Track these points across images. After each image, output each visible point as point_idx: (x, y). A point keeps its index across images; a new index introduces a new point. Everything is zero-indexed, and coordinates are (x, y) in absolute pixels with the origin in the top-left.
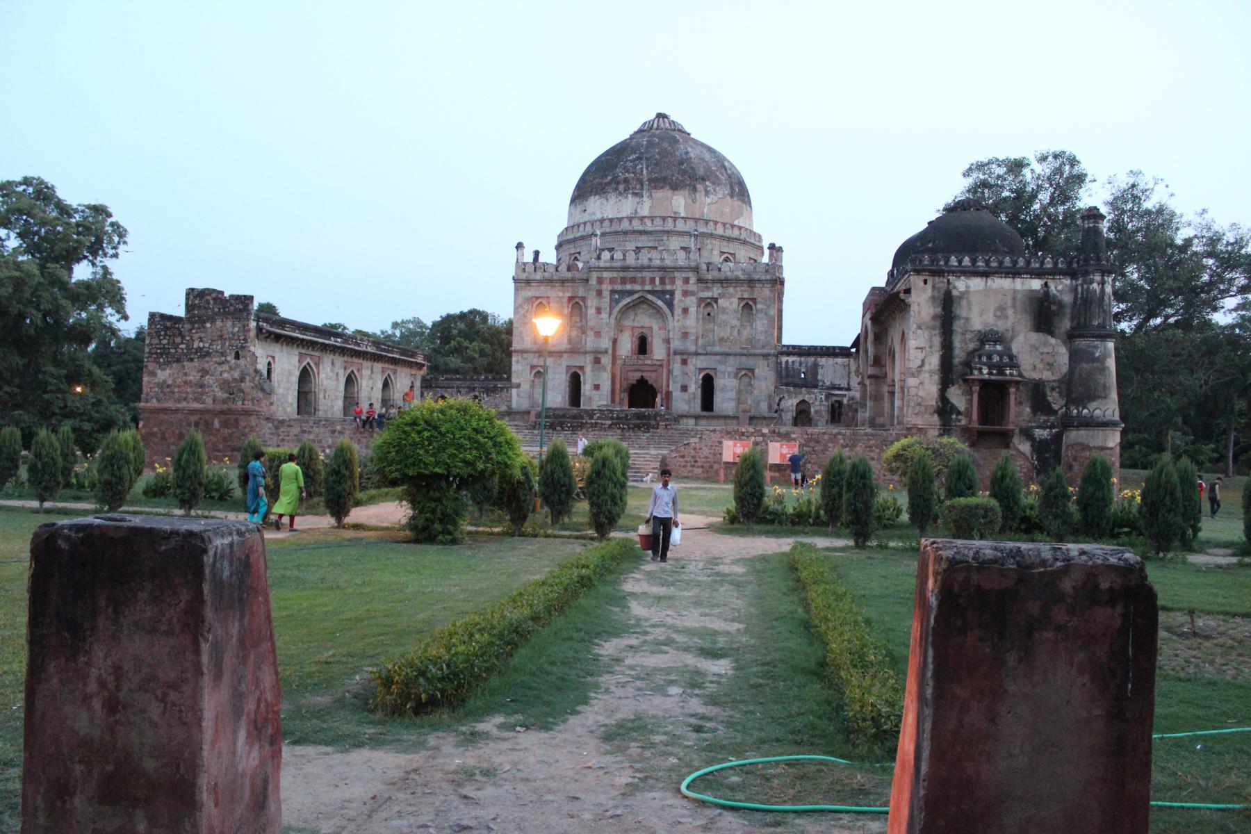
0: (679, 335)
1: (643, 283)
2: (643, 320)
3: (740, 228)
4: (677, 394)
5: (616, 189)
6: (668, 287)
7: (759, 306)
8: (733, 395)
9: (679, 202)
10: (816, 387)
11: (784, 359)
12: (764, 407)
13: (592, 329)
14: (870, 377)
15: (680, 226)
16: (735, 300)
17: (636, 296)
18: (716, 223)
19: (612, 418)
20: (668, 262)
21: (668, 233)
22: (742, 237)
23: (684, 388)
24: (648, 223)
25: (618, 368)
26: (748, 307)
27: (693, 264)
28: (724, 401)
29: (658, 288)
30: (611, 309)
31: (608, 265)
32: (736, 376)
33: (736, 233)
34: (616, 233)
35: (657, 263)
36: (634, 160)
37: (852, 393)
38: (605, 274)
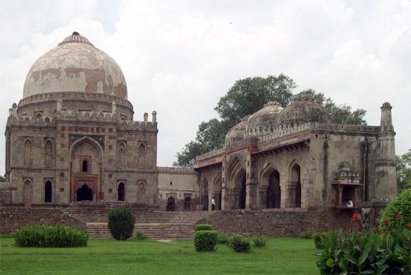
0: (107, 161)
1: (87, 131)
2: (86, 152)
4: (106, 193)
6: (102, 134)
7: (148, 146)
8: (135, 194)
12: (152, 200)
14: (250, 184)
15: (102, 99)
16: (136, 142)
17: (85, 137)
20: (101, 120)
21: (97, 102)
23: (110, 191)
24: (86, 97)
26: (142, 146)
27: (115, 121)
30: (70, 144)
31: (68, 119)
33: (126, 105)
34: (67, 101)
35: (95, 120)
38: (66, 125)
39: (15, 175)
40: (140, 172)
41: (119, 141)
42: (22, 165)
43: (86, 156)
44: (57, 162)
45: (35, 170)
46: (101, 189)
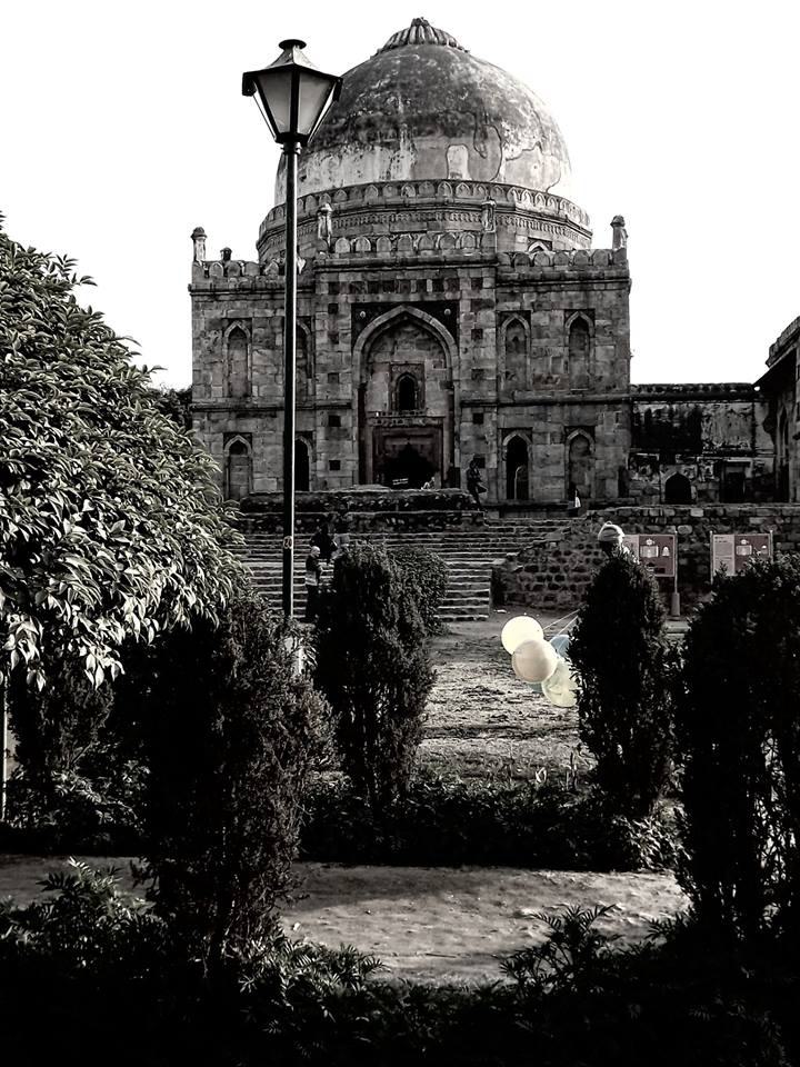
0: (468, 376)
2: (409, 352)
3: (558, 200)
5: (354, 139)
6: (448, 296)
8: (560, 470)
9: (460, 159)
10: (700, 454)
11: (643, 408)
12: (612, 487)
13: (324, 370)
15: (463, 195)
16: (560, 314)
17: (395, 312)
18: (520, 190)
19: (376, 507)
22: (562, 214)
24: (411, 193)
25: (369, 433)
26: (580, 328)
27: (488, 255)
28: (547, 483)
29: (432, 298)
30: (355, 334)
31: (347, 261)
32: (563, 440)
33: (551, 208)
36: (381, 90)
37: (759, 460)
38: (343, 278)
39: (202, 428)
40: (571, 403)
41: (502, 316)
42: (220, 401)
43: (407, 364)
44: (318, 386)
45: (257, 412)
46: (452, 460)
